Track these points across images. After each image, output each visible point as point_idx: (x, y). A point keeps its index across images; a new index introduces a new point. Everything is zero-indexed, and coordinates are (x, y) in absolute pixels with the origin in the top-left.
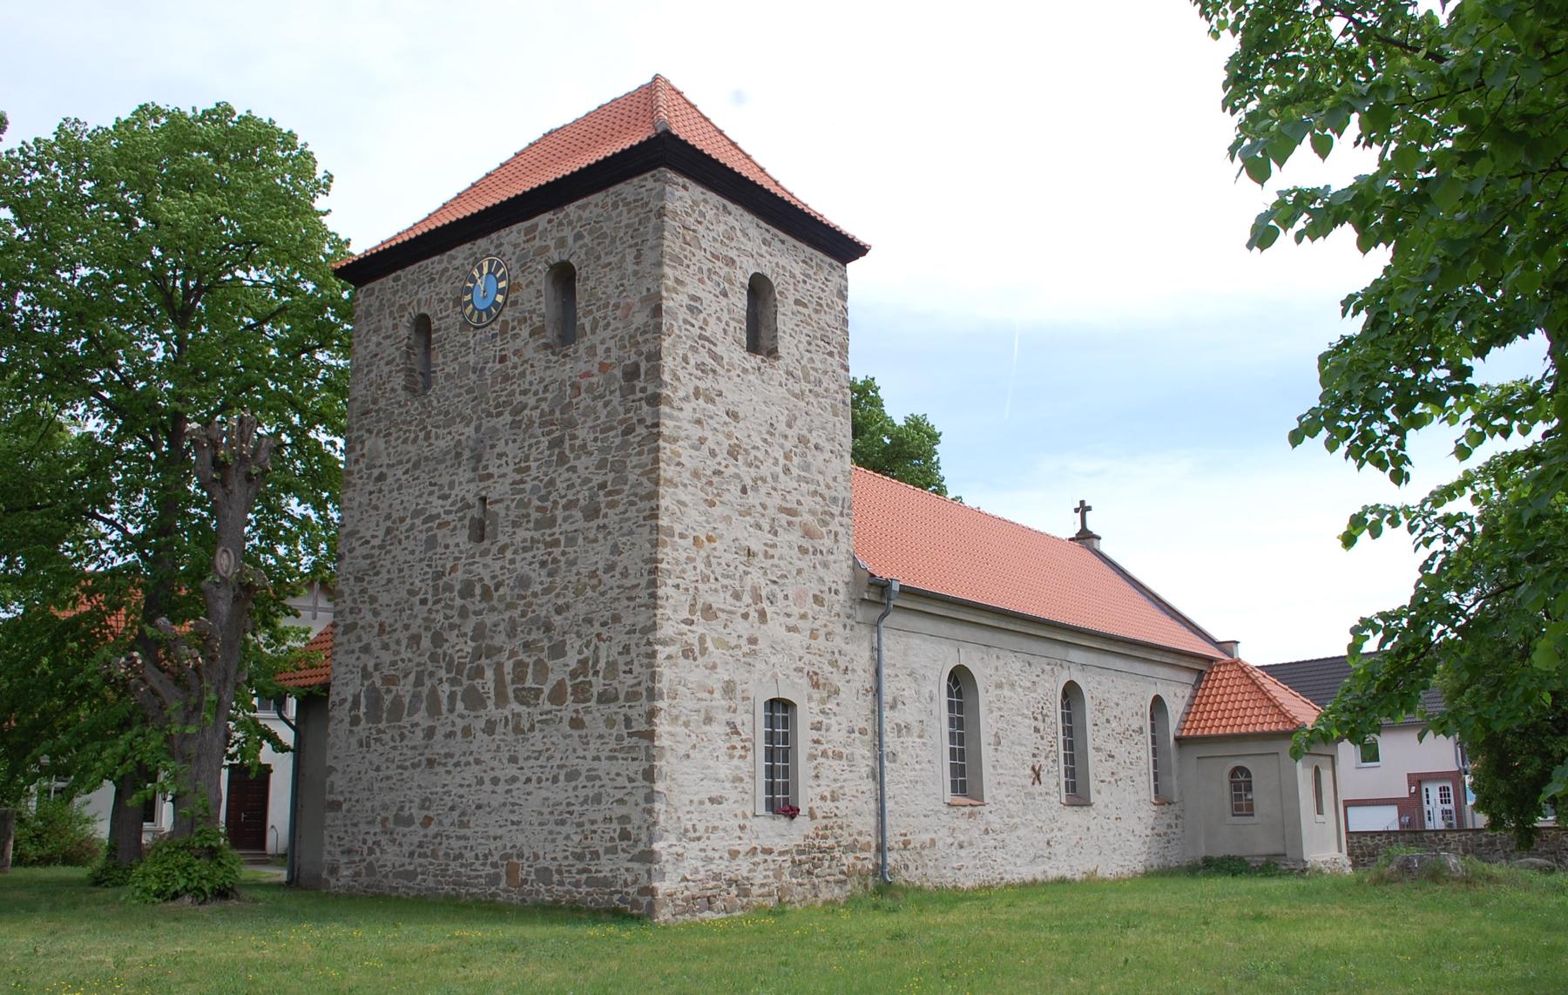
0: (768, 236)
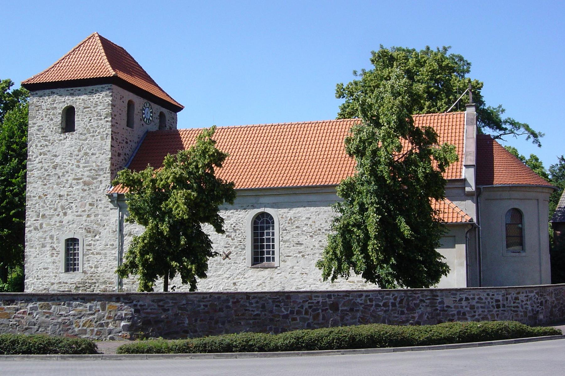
0: (72, 92)
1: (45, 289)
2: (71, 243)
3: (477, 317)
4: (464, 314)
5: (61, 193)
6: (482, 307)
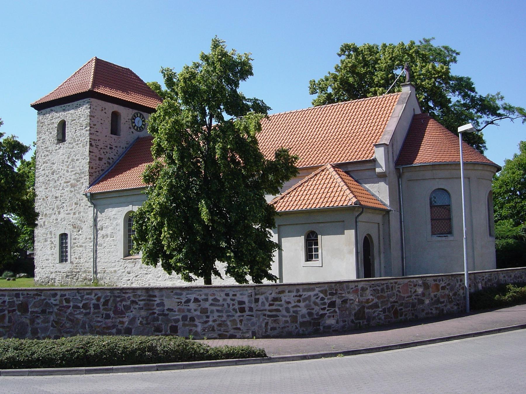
0: (64, 108)
1: (47, 277)
2: (63, 237)
3: (210, 323)
4: (192, 319)
5: (57, 195)
6: (218, 311)
